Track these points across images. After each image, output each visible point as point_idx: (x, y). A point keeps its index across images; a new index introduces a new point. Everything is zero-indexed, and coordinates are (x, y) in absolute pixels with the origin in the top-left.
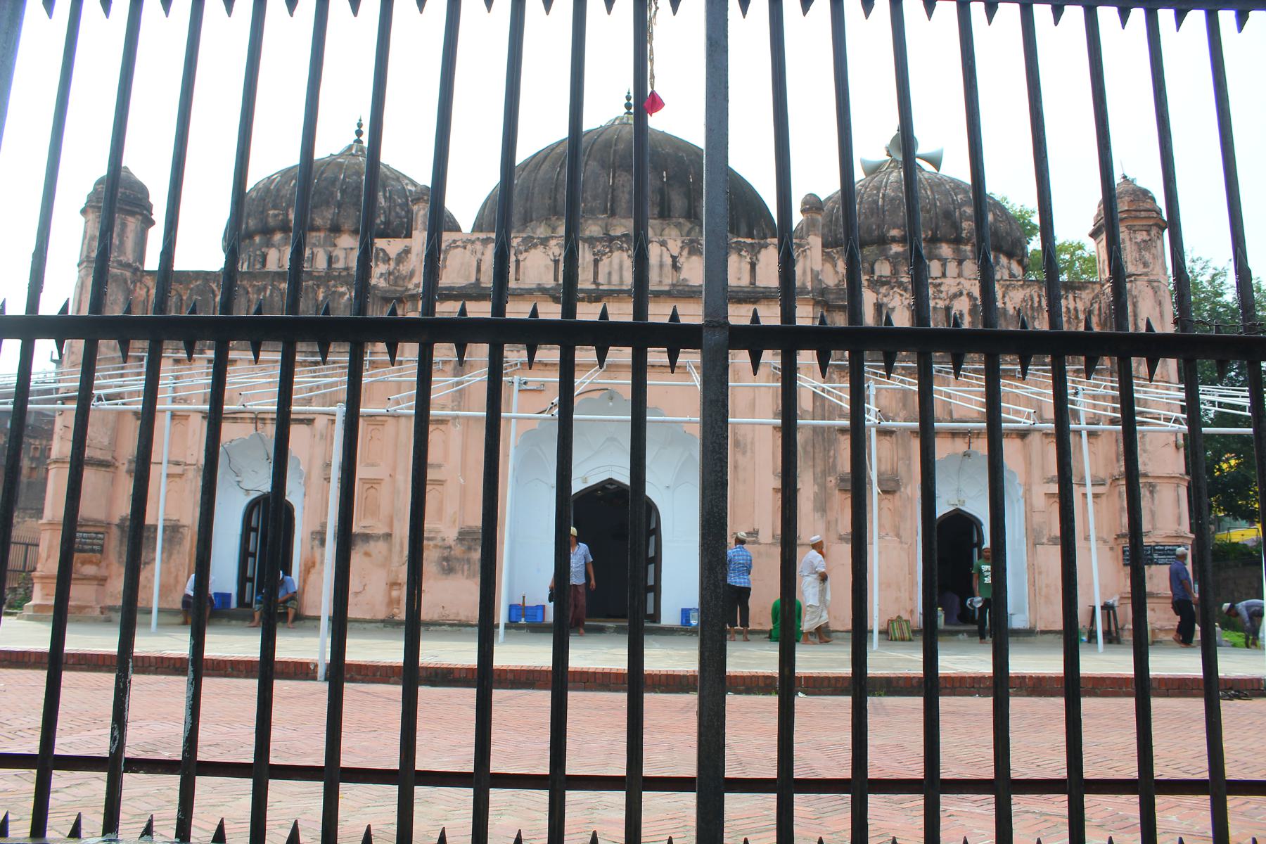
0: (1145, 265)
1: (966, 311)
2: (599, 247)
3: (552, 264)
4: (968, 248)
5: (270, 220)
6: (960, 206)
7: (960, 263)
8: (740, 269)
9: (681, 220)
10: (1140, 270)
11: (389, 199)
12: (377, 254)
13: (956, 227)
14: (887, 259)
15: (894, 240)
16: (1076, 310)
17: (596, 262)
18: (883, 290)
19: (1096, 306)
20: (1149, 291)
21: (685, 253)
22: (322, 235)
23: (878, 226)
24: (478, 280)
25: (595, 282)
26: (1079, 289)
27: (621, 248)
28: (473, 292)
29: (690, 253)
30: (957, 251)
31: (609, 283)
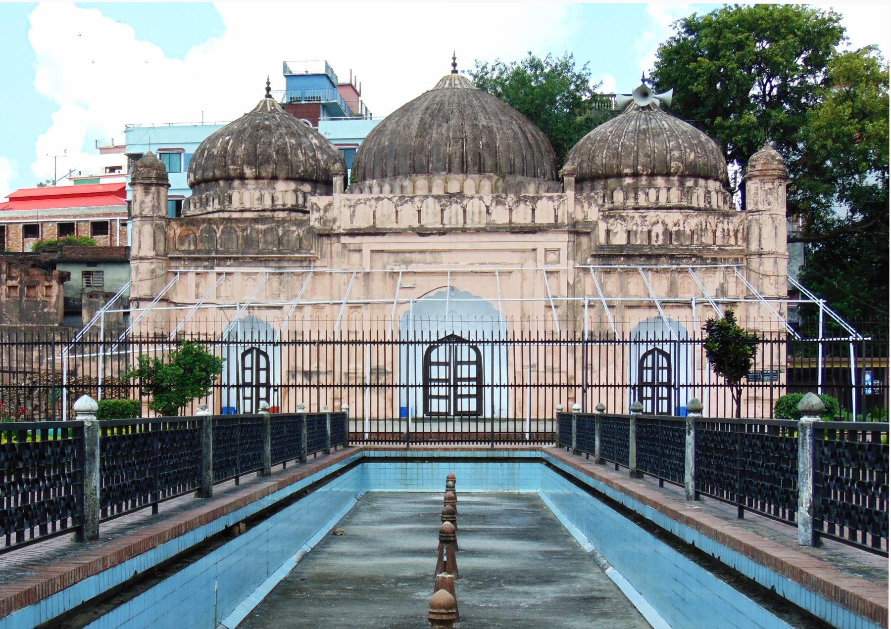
0: (769, 204)
1: (660, 233)
2: (443, 201)
4: (676, 178)
6: (671, 150)
8: (525, 213)
9: (492, 174)
10: (766, 207)
11: (305, 154)
12: (312, 207)
13: (668, 167)
14: (622, 189)
15: (627, 175)
16: (728, 230)
17: (442, 211)
18: (611, 221)
19: (741, 227)
20: (770, 220)
21: (494, 204)
22: (266, 181)
23: (618, 166)
25: (442, 223)
26: (732, 216)
27: (457, 202)
28: (372, 231)
29: (497, 204)
30: (667, 181)
31: (450, 223)
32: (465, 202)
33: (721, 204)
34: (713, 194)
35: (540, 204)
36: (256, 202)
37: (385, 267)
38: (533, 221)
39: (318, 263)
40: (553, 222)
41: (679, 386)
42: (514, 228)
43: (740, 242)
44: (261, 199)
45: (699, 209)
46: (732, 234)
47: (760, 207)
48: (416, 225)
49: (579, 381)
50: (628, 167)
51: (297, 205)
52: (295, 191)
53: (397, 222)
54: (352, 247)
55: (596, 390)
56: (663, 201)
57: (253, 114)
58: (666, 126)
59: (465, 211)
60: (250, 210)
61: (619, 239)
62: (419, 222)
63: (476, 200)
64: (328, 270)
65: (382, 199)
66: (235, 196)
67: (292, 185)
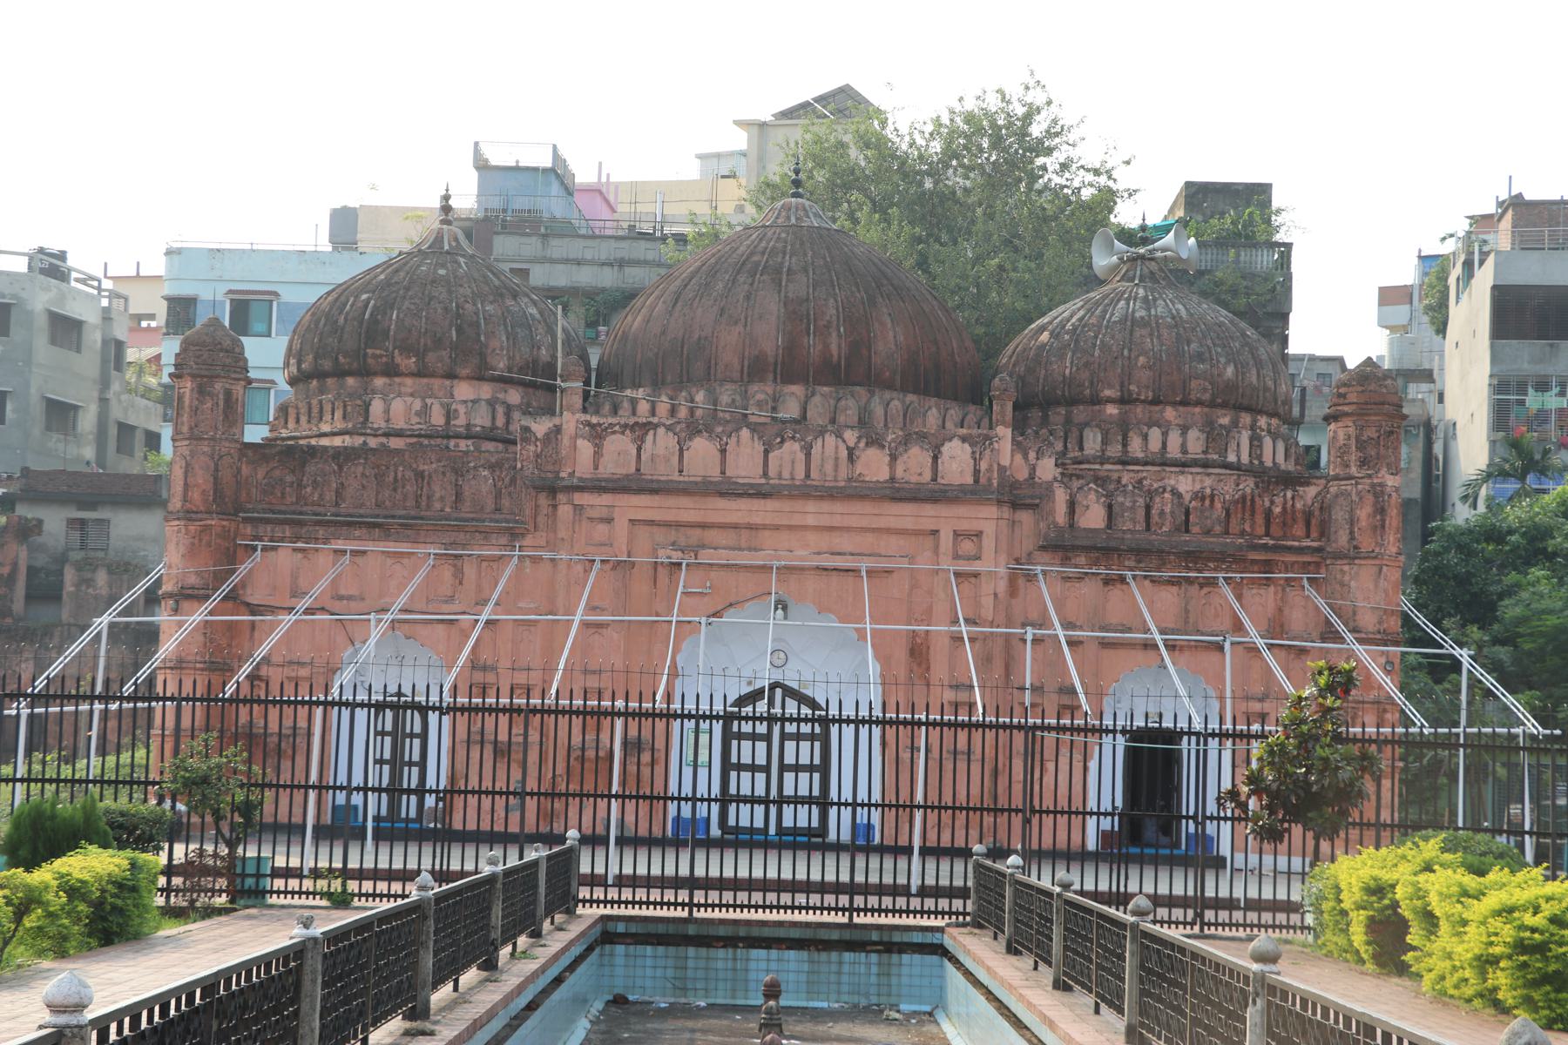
1: (1168, 509)
3: (718, 454)
5: (370, 361)
7: (1184, 430)
15: (1110, 400)
17: (766, 452)
18: (1076, 484)
20: (1370, 498)
21: (862, 445)
24: (638, 470)
25: (765, 474)
26: (1302, 485)
29: (867, 444)
32: (809, 438)
33: (1280, 458)
34: (1268, 442)
35: (947, 449)
36: (415, 420)
37: (655, 554)
38: (934, 479)
39: (528, 541)
40: (970, 480)
41: (1205, 817)
42: (898, 490)
43: (1314, 534)
44: (425, 411)
45: (1236, 467)
46: (1299, 516)
47: (1354, 470)
48: (714, 473)
49: (1017, 802)
50: (1111, 387)
51: (494, 427)
52: (492, 403)
53: (681, 471)
54: (595, 514)
55: (1048, 821)
56: (1174, 451)
57: (418, 253)
58: (1183, 313)
59: (808, 455)
60: (399, 434)
61: (1093, 517)
62: (723, 472)
63: (830, 440)
64: (547, 555)
65: (655, 426)
66: (377, 407)
67: (486, 391)
